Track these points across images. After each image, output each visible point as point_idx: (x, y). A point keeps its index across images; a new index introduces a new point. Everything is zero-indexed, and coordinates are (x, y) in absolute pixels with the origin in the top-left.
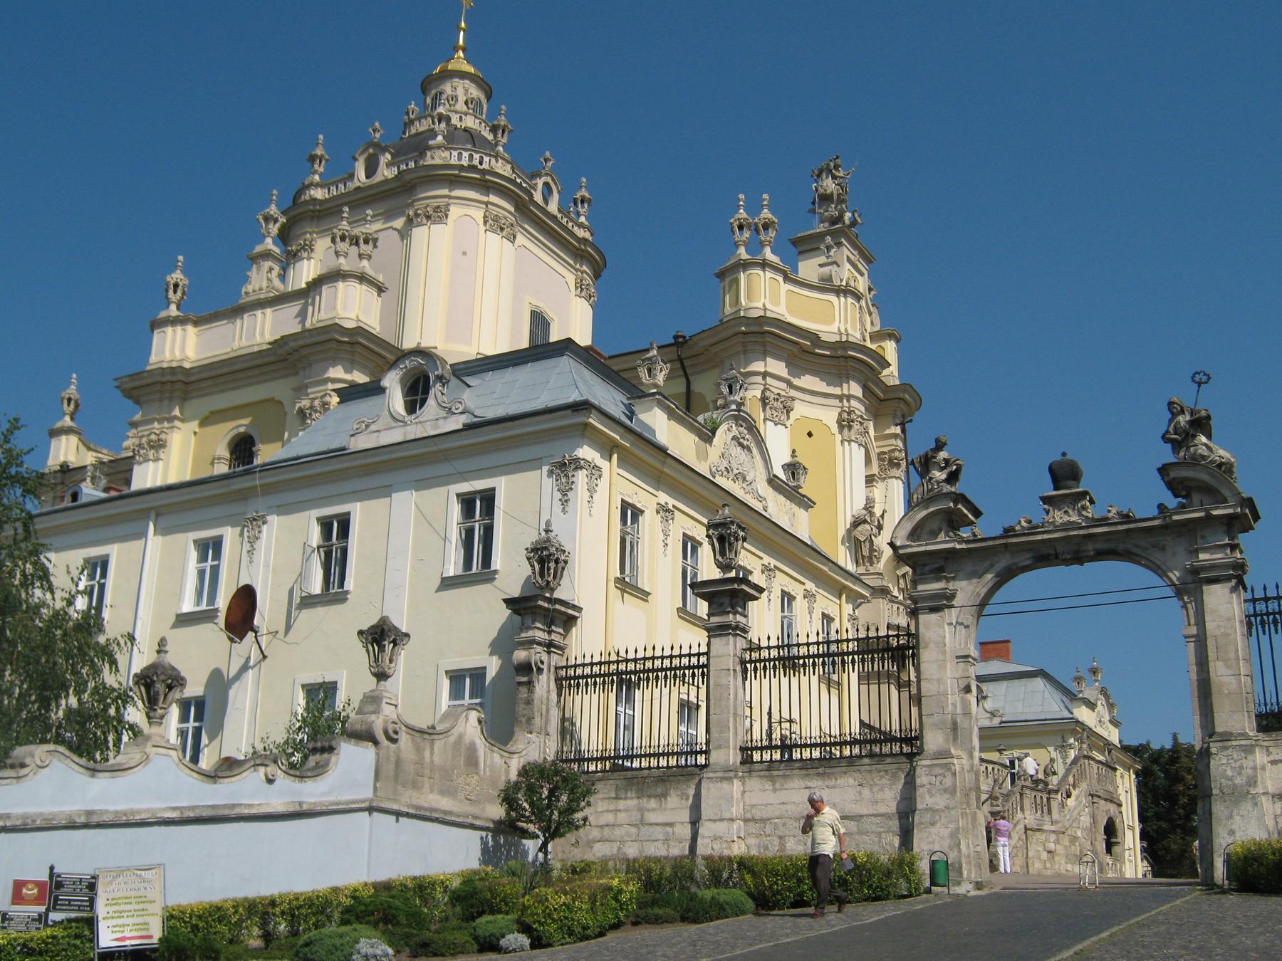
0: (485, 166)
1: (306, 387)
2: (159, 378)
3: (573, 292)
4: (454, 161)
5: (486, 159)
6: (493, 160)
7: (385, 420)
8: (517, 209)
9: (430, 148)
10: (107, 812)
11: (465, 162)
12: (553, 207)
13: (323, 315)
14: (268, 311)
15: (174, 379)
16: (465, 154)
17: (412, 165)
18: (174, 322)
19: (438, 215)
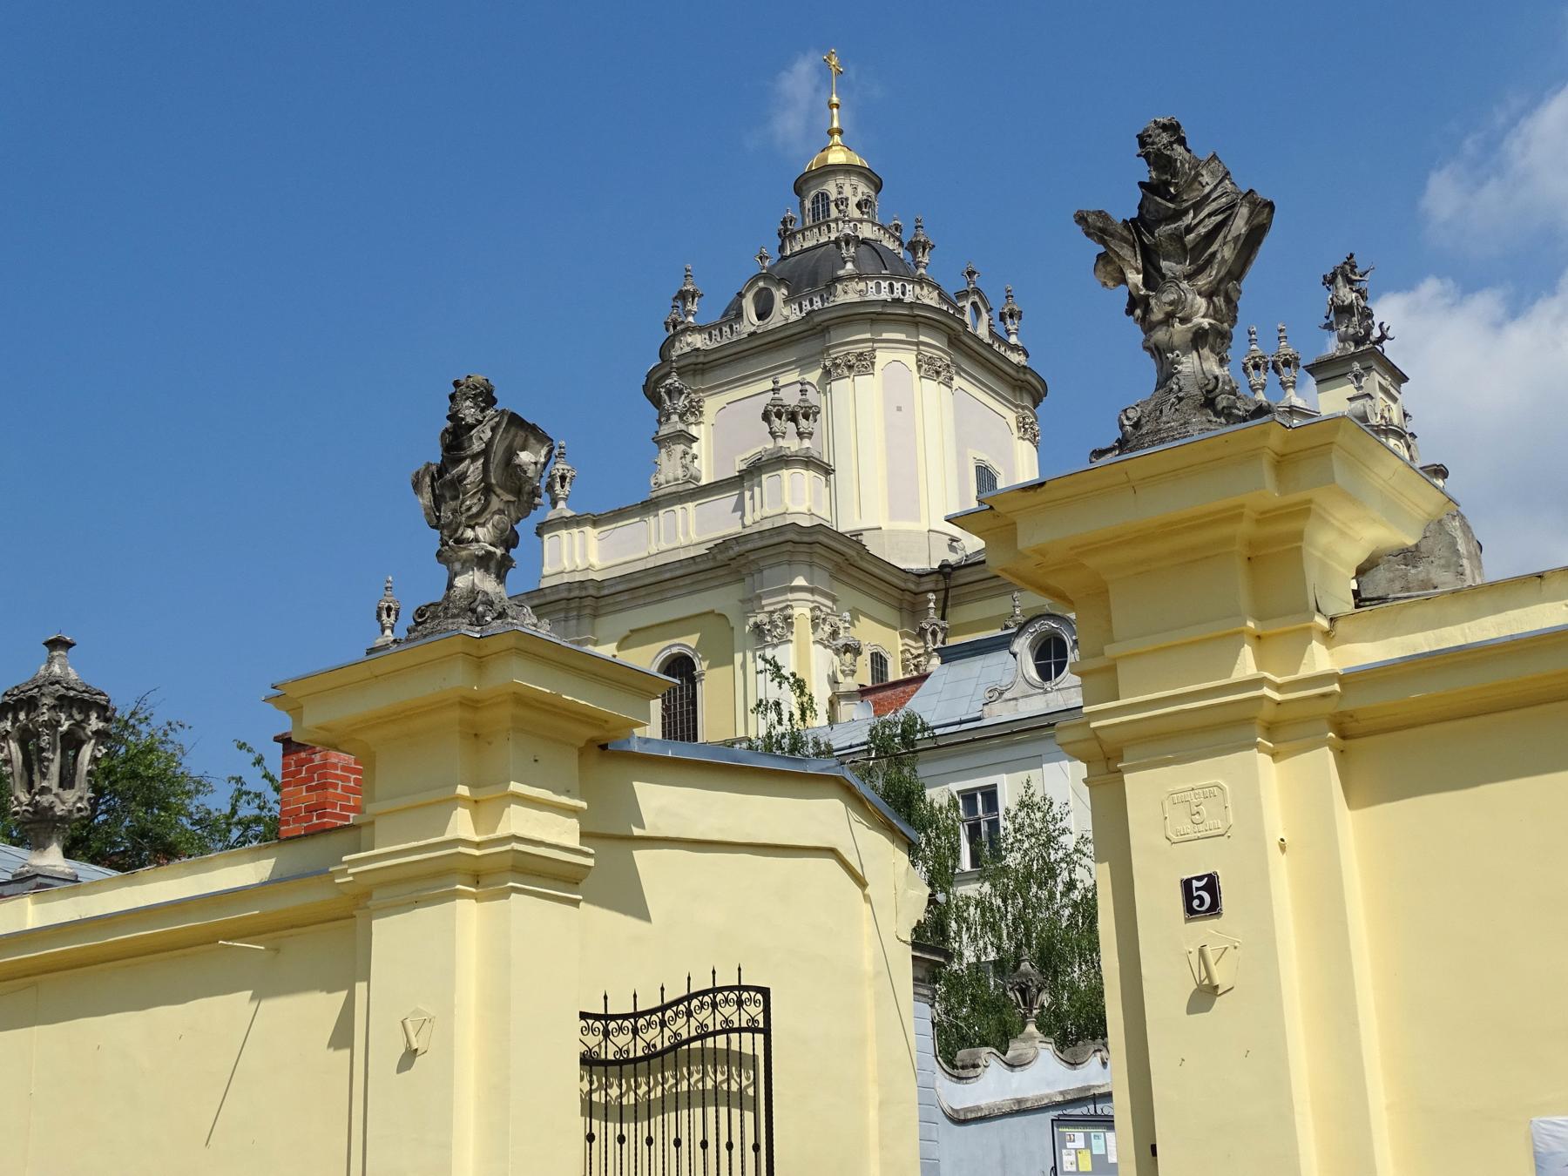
0: (908, 299)
1: (760, 598)
2: (564, 595)
3: (1016, 434)
4: (872, 296)
5: (909, 287)
6: (917, 288)
7: (1021, 688)
8: (951, 343)
9: (840, 279)
10: (1027, 1100)
11: (885, 295)
12: (983, 331)
13: (767, 511)
14: (690, 506)
15: (584, 594)
16: (885, 284)
17: (818, 304)
18: (566, 523)
19: (863, 364)
